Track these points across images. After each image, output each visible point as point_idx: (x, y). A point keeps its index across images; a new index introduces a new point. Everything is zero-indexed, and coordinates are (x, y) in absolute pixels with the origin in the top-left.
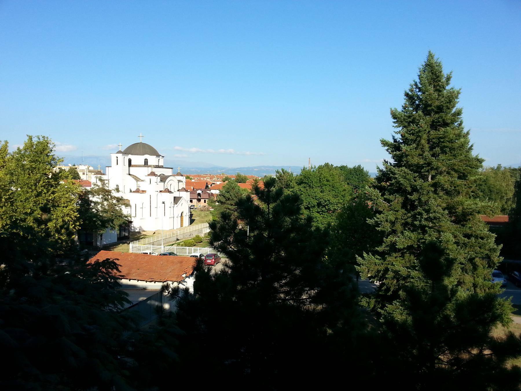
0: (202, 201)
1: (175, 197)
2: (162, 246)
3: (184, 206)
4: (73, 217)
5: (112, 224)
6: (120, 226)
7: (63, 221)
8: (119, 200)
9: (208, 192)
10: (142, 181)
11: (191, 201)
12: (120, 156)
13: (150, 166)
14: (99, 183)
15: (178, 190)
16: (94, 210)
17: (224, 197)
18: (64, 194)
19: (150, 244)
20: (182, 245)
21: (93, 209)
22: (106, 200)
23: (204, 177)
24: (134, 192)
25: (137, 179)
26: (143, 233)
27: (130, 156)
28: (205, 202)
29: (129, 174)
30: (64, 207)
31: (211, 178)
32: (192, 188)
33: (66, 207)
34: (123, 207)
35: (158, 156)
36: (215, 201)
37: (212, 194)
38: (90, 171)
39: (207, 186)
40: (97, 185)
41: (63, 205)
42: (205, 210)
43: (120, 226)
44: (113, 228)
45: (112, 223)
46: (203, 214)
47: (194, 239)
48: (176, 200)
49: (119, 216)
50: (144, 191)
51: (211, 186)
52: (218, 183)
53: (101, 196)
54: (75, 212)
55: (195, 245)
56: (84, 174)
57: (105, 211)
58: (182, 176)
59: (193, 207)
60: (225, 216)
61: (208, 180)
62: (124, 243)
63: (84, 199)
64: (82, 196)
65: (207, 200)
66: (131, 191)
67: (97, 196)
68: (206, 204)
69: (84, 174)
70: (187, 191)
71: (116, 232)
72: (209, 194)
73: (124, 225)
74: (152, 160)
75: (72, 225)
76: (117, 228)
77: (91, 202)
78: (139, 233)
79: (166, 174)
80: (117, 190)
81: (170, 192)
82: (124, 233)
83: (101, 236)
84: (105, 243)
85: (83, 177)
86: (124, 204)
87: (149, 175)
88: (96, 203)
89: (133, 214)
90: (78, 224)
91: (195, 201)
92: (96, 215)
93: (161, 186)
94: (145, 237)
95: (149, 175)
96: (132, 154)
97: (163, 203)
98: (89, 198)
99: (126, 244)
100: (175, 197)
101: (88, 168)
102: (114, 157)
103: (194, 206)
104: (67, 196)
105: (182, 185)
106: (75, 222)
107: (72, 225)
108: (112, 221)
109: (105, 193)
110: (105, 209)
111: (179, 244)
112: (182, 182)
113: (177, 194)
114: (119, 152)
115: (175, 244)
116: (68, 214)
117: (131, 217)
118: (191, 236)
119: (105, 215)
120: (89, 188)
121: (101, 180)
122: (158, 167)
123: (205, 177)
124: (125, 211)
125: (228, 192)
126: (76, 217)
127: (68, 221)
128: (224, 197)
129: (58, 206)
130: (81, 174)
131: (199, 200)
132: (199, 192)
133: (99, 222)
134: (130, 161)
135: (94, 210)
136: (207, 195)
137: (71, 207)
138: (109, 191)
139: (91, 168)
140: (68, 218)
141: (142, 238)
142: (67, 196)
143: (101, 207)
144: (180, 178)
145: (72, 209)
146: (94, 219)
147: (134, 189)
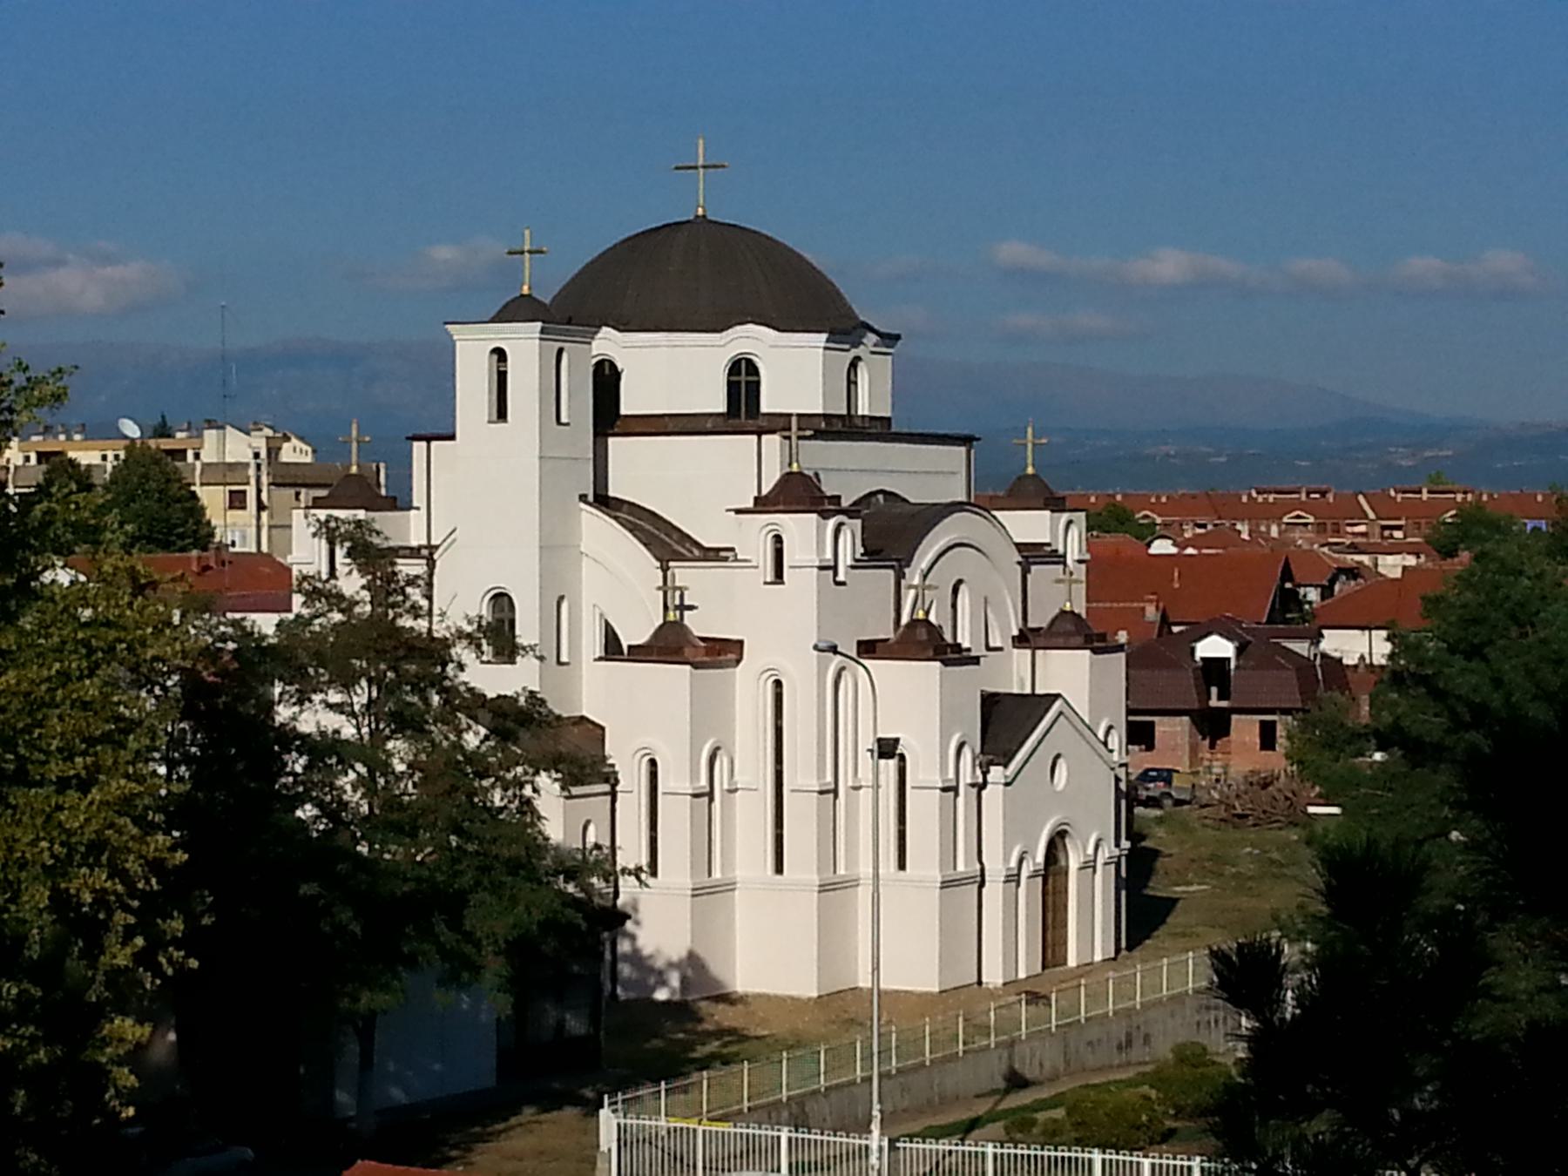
0: (1245, 729)
1: (991, 702)
2: (876, 1139)
3: (1076, 782)
4: (132, 865)
5: (446, 936)
6: (520, 950)
7: (61, 902)
8: (517, 721)
9: (1301, 647)
10: (714, 555)
11: (1140, 735)
12: (524, 343)
13: (778, 424)
14: (351, 583)
15: (1025, 639)
16: (306, 812)
17: (1438, 695)
18: (65, 676)
19: (769, 1113)
20: (1052, 1136)
21: (300, 801)
22: (408, 723)
23: (1257, 514)
24: (639, 654)
25: (665, 541)
26: (723, 1016)
27: (608, 343)
28: (1268, 738)
29: (603, 501)
30: (63, 784)
31: (1328, 525)
32: (1151, 613)
33: (84, 786)
34: (547, 793)
35: (844, 329)
36: (1359, 739)
37: (1333, 664)
38: (288, 478)
39: (1288, 601)
40: (337, 600)
41: (55, 769)
42: (1265, 819)
43: (520, 950)
44: (460, 970)
45: (455, 923)
46: (1246, 850)
47: (1157, 1079)
48: (1005, 724)
49: (514, 866)
50: (724, 652)
51: (1327, 592)
52: (1391, 566)
53: (360, 698)
54: (149, 828)
55: (1167, 1136)
56: (237, 501)
57: (393, 820)
58: (1056, 504)
59: (1155, 789)
60: (1360, 884)
61: (1300, 538)
62: (551, 1102)
63: (227, 707)
64: (214, 690)
65: (1283, 725)
66: (612, 648)
67: (335, 697)
68: (1276, 761)
69: (237, 501)
70: (1098, 643)
71: (486, 1003)
72: (1303, 666)
73: (550, 945)
74: (796, 371)
75: (129, 934)
76: (495, 967)
77: (289, 738)
78: (680, 1010)
79: (917, 493)
80: (499, 635)
81: (951, 654)
82: (551, 1014)
83: (366, 1027)
84: (398, 1095)
85: (236, 530)
86: (552, 763)
87: (763, 504)
88: (323, 749)
89: (631, 853)
90: (177, 925)
91: (1173, 731)
92: (325, 854)
93: (873, 603)
94: (733, 1047)
95: (763, 504)
96: (623, 326)
97: (887, 748)
98: (269, 707)
99: (570, 1113)
100: (991, 702)
101: (273, 452)
102: (471, 351)
103: (1166, 776)
104: (91, 688)
105: (1059, 593)
106: (151, 910)
107: (129, 934)
108: (453, 905)
109: (396, 657)
110: (394, 804)
111: (1019, 1126)
112: (1058, 558)
113: (1015, 673)
114: (516, 310)
115: (992, 1117)
116: (97, 846)
117: (611, 876)
118: (1137, 1053)
119: (393, 853)
120: (266, 623)
121: (371, 556)
122: (839, 427)
123: (1274, 513)
124: (558, 815)
125: (1474, 652)
126: (155, 866)
127: (101, 897)
128: (1438, 695)
129: (21, 777)
130: (212, 499)
131: (1213, 726)
132: (1216, 647)
133: (345, 915)
134: (607, 379)
135: (306, 812)
136: (1291, 675)
137: (119, 786)
138: (435, 651)
139: (294, 452)
140: (101, 878)
141: (704, 1064)
142: (91, 688)
143: (366, 784)
144: (1031, 525)
145: (125, 804)
146: (306, 889)
147: (634, 634)
